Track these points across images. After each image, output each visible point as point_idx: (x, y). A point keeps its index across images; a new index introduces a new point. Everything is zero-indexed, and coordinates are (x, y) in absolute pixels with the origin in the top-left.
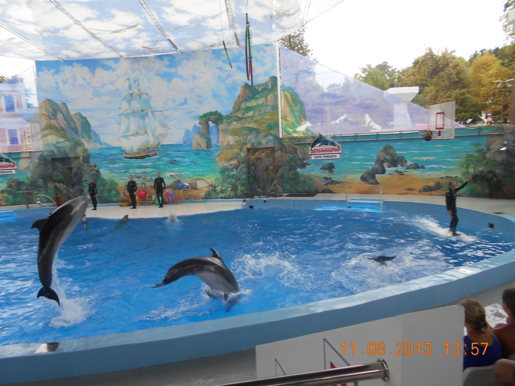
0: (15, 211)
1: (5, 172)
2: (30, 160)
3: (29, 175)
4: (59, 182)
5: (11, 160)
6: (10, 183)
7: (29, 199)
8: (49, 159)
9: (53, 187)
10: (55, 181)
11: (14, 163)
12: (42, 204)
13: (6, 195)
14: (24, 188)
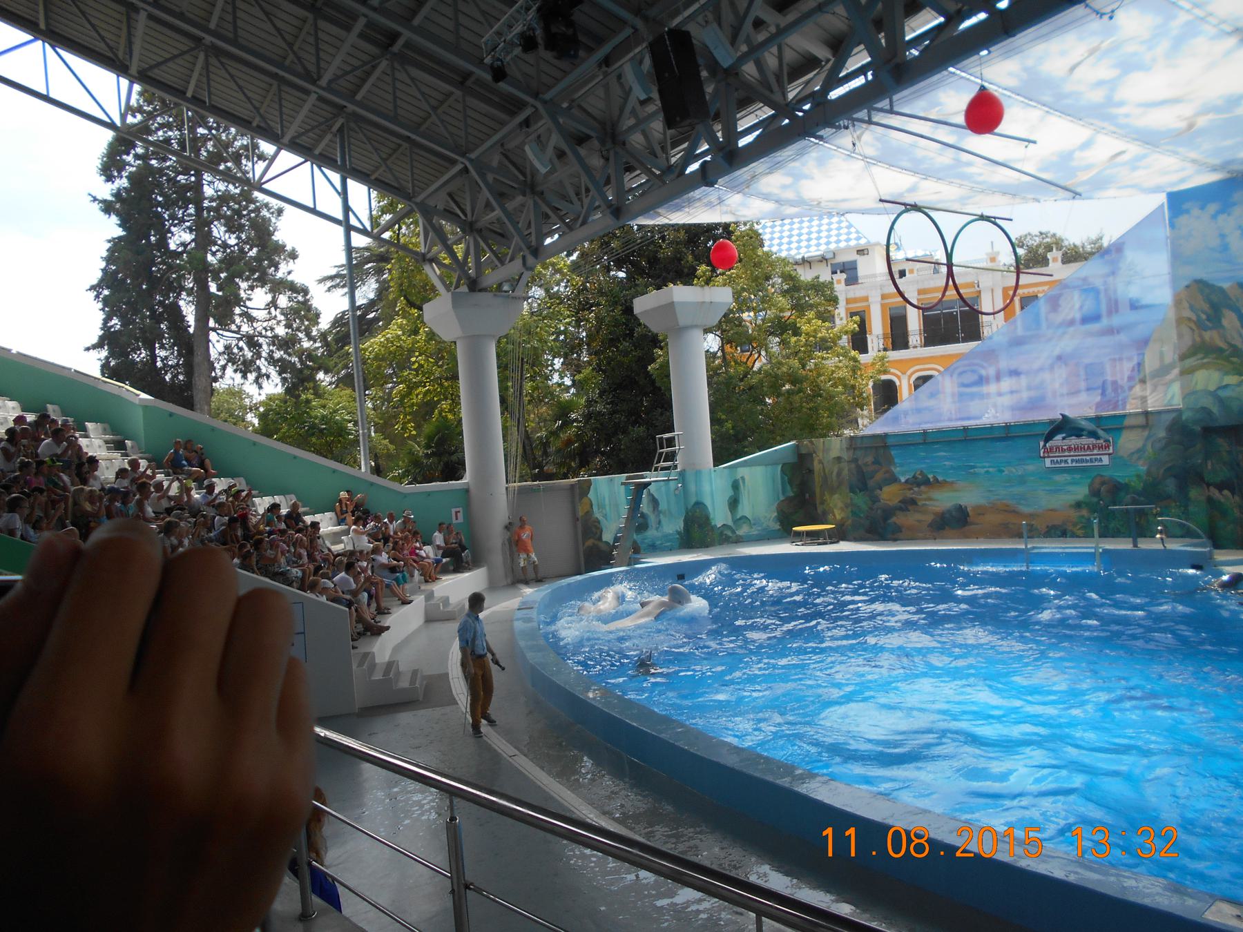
0: (1105, 551)
1: (1087, 461)
2: (1146, 433)
3: (1143, 468)
4: (1220, 490)
5: (1101, 433)
7: (1137, 523)
8: (1198, 428)
10: (1208, 485)
13: (1085, 512)
14: (1128, 498)
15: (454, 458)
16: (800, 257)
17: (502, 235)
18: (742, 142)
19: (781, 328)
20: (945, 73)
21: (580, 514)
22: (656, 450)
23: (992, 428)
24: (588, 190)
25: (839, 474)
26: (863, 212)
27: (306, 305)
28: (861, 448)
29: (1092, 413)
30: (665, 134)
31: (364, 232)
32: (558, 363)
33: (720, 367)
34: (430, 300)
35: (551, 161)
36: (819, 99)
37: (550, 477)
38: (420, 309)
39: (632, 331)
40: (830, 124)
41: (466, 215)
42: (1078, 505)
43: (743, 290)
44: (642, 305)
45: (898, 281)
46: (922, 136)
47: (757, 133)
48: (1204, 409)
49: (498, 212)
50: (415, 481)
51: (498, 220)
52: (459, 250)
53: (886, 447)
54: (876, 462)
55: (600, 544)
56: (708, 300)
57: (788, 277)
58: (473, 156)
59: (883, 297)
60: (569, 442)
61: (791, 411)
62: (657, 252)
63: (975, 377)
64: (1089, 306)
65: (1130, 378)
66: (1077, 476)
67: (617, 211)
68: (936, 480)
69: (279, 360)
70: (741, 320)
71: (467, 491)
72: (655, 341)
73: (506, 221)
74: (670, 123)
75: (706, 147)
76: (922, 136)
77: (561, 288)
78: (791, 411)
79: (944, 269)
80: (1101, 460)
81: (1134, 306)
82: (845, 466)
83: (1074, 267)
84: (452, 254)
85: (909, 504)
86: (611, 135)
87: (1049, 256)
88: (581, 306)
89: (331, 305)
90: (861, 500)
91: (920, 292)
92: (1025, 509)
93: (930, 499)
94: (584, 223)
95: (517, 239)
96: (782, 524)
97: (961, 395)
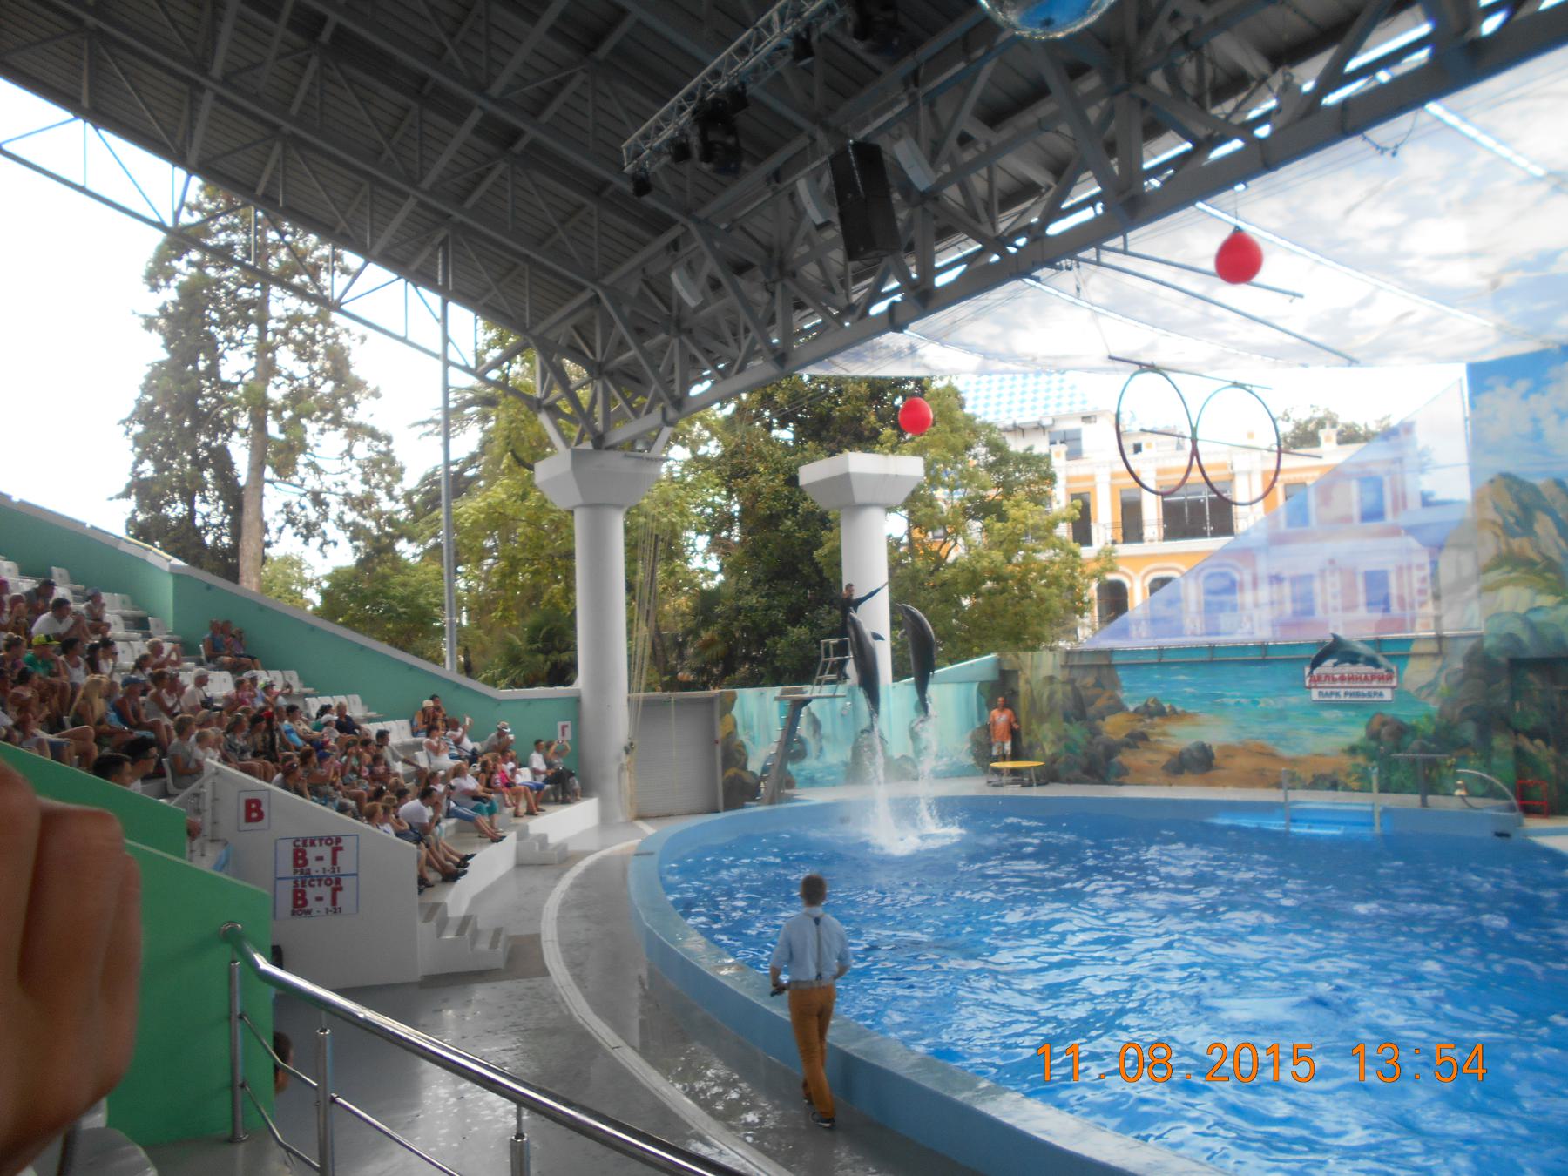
0: (1386, 811)
2: (1438, 663)
3: (1433, 706)
4: (1532, 735)
5: (1381, 660)
6: (1376, 727)
7: (1427, 778)
8: (1503, 660)
9: (1510, 748)
10: (1516, 732)
11: (1388, 670)
12: (1474, 801)
13: (1360, 759)
14: (1415, 744)
15: (565, 657)
16: (1009, 423)
17: (638, 381)
18: (940, 281)
19: (983, 509)
20: (1191, 209)
21: (720, 735)
22: (819, 658)
23: (1244, 648)
24: (747, 330)
25: (1051, 696)
26: (1090, 370)
27: (387, 456)
28: (1079, 667)
29: (1370, 634)
30: (845, 266)
31: (466, 369)
32: (702, 542)
33: (905, 556)
34: (544, 457)
35: (703, 292)
36: (1036, 234)
37: (687, 686)
38: (531, 468)
39: (796, 506)
40: (1050, 263)
41: (594, 353)
42: (1353, 750)
43: (937, 462)
44: (810, 474)
45: (1130, 457)
46: (1162, 283)
47: (962, 268)
48: (1511, 636)
49: (633, 352)
50: (514, 684)
51: (635, 361)
52: (584, 395)
53: (1111, 666)
54: (1098, 684)
55: (744, 774)
56: (892, 471)
57: (996, 447)
58: (606, 281)
59: (1114, 476)
60: (708, 645)
61: (993, 616)
62: (831, 409)
63: (1225, 583)
64: (1370, 498)
65: (1422, 592)
66: (1352, 713)
67: (781, 358)
68: (1174, 711)
69: (349, 525)
70: (932, 499)
71: (577, 700)
72: (822, 522)
73: (643, 362)
74: (851, 254)
75: (895, 284)
76: (1162, 283)
77: (713, 449)
78: (993, 616)
79: (1188, 445)
80: (1381, 695)
81: (1426, 501)
82: (1059, 688)
83: (1352, 449)
84: (575, 401)
85: (1138, 739)
86: (779, 267)
87: (1322, 434)
88: (733, 470)
89: (420, 459)
90: (1077, 732)
91: (1160, 472)
92: (1286, 753)
93: (1164, 734)
94: (741, 369)
95: (655, 386)
96: (976, 757)
97: (1208, 604)
